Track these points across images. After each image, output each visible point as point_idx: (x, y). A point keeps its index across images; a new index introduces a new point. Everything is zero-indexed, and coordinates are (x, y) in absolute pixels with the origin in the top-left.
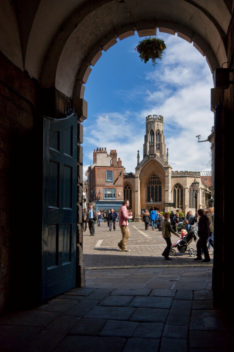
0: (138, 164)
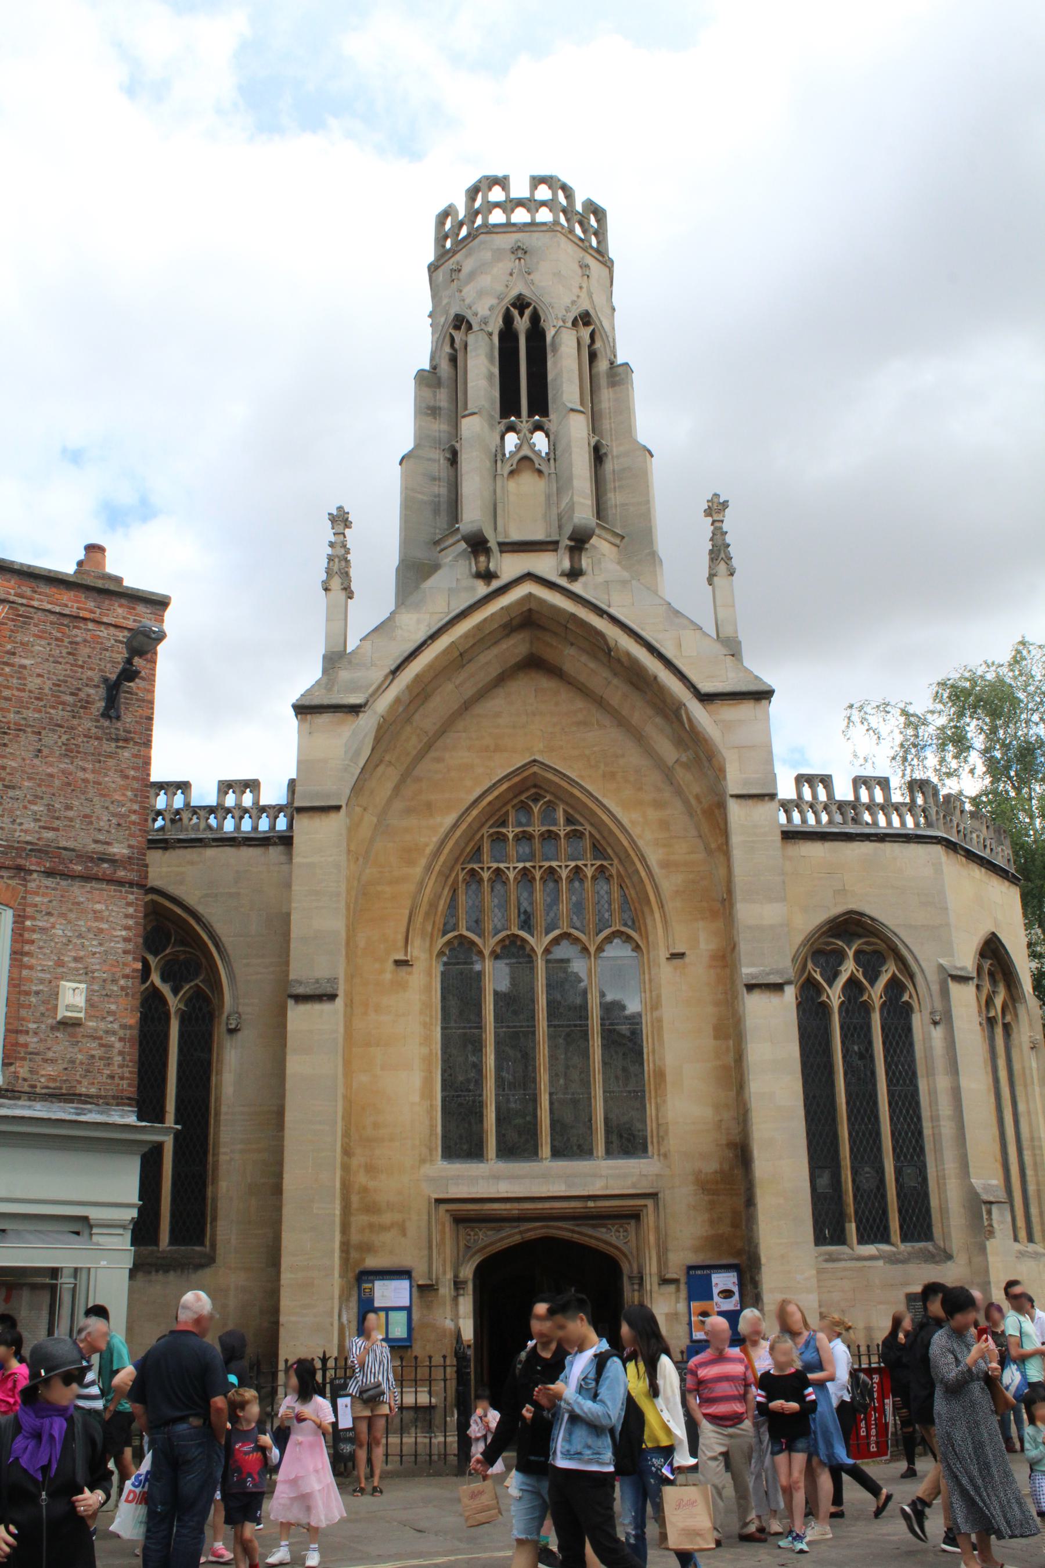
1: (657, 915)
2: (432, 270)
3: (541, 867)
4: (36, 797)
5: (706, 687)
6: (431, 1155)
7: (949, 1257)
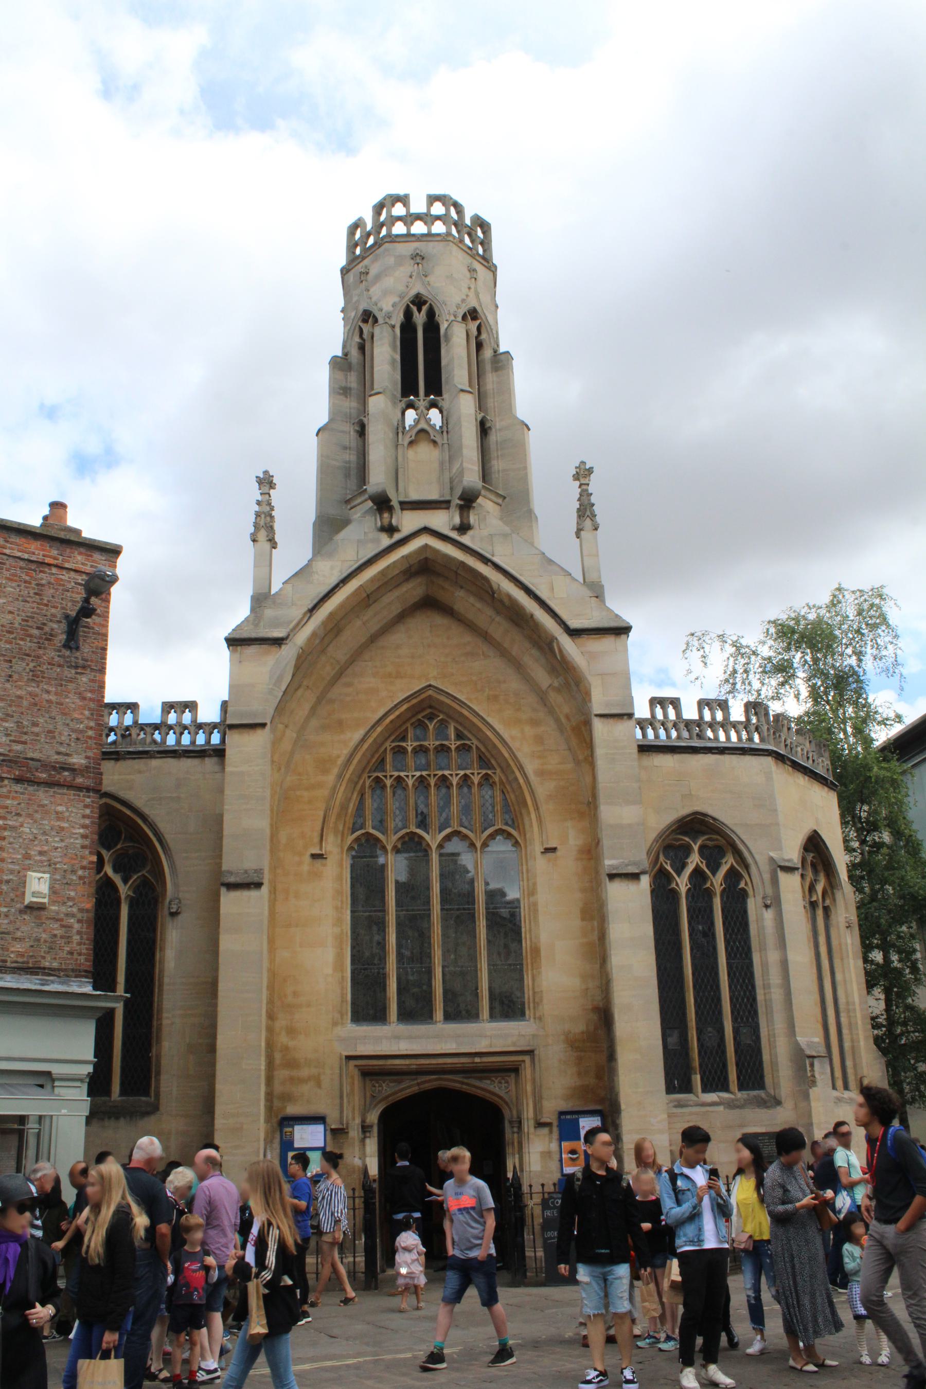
0: (260, 600)
1: (533, 816)
2: (344, 272)
3: (435, 775)
4: (8, 715)
5: (574, 624)
6: (342, 1018)
7: (778, 1103)
